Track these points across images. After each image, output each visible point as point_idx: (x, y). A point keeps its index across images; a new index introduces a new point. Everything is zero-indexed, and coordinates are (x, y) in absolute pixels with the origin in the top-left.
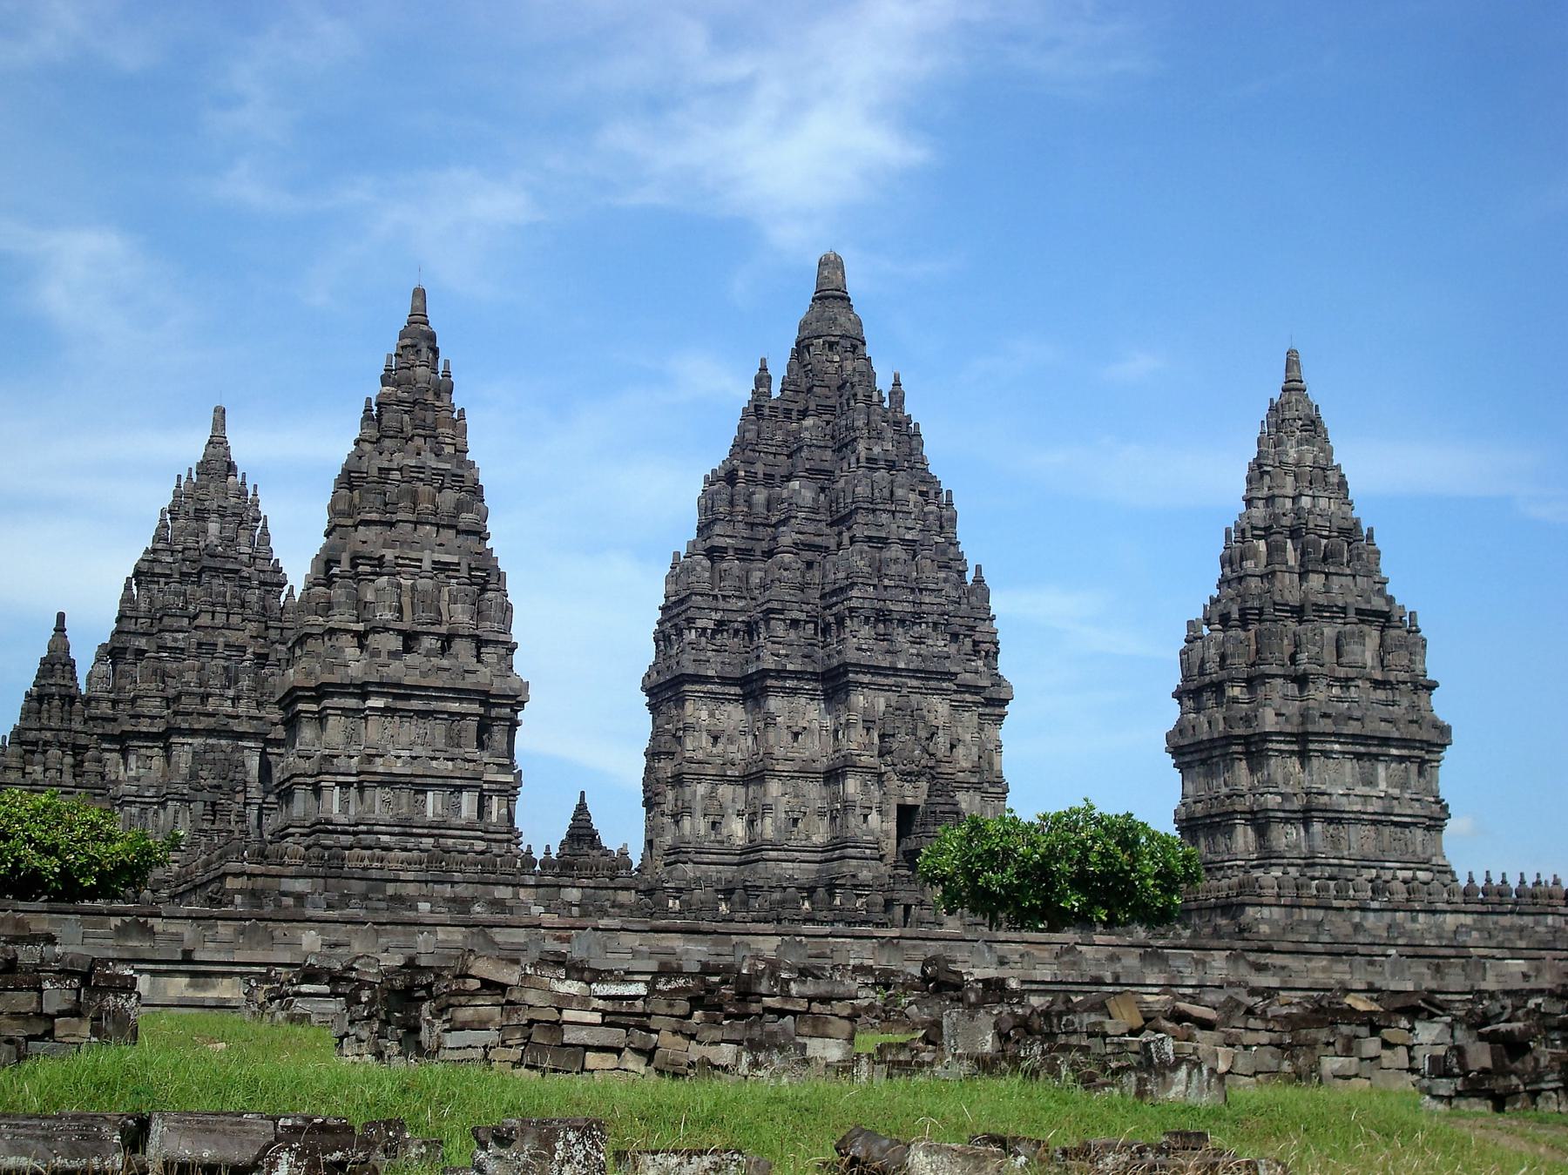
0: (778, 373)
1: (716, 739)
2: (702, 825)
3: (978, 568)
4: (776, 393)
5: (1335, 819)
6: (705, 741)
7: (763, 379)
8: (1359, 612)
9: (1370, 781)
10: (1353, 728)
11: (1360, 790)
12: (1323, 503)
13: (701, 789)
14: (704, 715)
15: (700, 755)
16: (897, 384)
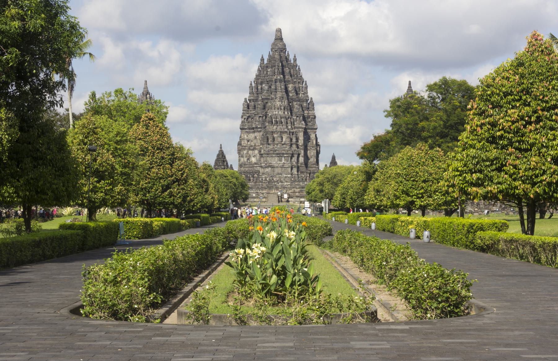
0: (266, 58)
1: (248, 141)
2: (245, 159)
3: (311, 98)
4: (266, 62)
5: (273, 167)
6: (246, 142)
7: (262, 60)
8: (281, 132)
9: (281, 161)
10: (277, 152)
11: (279, 162)
12: (280, 112)
13: (245, 152)
14: (246, 136)
15: (245, 145)
16: (295, 57)
